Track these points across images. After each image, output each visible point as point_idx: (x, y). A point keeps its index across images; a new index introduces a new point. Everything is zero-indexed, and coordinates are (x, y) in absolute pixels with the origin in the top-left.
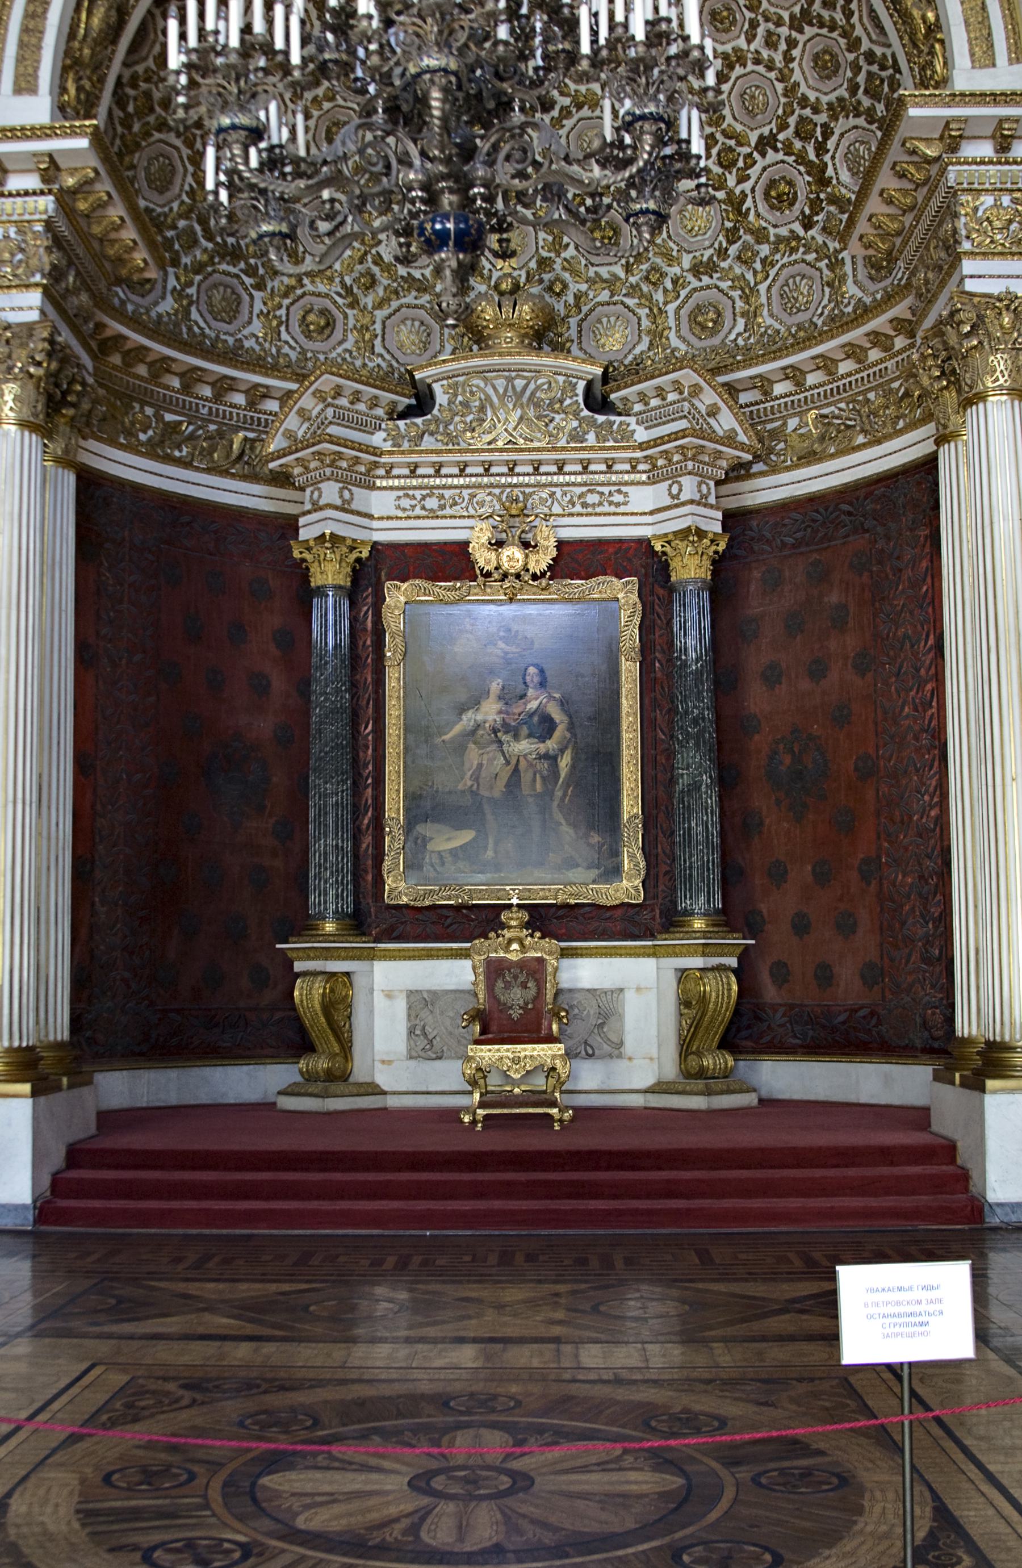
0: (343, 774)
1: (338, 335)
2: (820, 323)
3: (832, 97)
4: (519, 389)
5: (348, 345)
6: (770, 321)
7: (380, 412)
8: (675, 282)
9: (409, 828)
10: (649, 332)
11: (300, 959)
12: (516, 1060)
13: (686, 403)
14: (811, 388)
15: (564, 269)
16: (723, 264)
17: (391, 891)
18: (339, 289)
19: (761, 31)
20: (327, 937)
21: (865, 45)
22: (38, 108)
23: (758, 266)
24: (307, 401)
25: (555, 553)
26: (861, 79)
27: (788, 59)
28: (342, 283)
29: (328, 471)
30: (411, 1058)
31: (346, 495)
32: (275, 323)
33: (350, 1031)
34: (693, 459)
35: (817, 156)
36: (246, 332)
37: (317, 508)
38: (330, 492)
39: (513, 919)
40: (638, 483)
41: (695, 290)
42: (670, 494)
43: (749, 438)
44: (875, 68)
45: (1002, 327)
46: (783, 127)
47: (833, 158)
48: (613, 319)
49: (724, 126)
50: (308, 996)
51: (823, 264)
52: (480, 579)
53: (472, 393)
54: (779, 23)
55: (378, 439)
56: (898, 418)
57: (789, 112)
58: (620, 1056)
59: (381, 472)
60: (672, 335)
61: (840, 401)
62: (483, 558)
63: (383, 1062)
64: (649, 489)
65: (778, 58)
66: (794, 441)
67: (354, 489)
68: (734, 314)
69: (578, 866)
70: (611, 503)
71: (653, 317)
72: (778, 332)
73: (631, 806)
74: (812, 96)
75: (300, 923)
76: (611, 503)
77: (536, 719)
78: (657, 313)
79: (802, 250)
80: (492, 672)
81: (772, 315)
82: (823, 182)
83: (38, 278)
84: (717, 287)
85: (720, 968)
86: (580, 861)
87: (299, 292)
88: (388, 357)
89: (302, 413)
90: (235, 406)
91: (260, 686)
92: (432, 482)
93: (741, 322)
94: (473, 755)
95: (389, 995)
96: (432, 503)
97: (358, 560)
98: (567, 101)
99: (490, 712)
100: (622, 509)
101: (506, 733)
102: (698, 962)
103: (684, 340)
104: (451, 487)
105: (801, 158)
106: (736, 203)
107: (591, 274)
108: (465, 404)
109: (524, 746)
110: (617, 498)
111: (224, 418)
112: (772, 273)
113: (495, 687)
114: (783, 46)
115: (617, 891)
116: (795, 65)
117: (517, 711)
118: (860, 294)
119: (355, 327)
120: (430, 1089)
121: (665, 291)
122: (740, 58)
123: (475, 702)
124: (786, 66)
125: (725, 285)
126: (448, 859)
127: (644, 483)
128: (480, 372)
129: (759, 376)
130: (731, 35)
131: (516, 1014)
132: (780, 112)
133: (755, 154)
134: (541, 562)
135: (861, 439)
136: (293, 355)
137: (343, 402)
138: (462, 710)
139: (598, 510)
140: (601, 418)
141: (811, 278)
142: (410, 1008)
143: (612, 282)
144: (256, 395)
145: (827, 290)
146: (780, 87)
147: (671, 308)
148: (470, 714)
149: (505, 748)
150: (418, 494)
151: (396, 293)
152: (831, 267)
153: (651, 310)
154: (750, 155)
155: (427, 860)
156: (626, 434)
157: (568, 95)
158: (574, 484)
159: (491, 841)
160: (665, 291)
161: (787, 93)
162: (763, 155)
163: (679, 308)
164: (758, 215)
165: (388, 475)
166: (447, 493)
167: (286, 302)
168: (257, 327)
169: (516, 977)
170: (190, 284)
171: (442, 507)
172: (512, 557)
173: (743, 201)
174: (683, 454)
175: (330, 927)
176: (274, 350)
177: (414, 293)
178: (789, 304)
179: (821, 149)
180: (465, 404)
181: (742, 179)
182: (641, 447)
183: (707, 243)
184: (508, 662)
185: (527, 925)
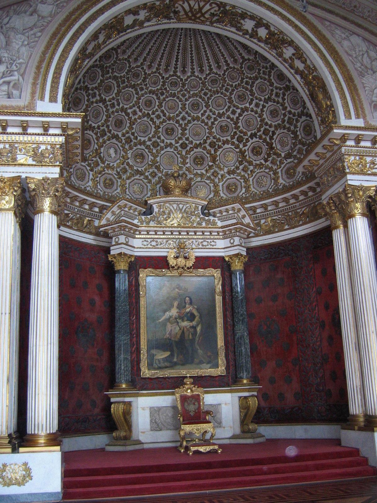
0: (127, 333)
1: (115, 187)
2: (271, 190)
3: (276, 123)
4: (181, 208)
5: (118, 191)
6: (253, 190)
7: (136, 213)
8: (222, 176)
9: (148, 351)
11: (113, 397)
12: (197, 430)
13: (236, 214)
14: (269, 211)
15: (186, 170)
16: (238, 171)
17: (143, 373)
18: (115, 173)
19: (254, 102)
20: (124, 389)
21: (288, 109)
22: (58, 107)
23: (249, 172)
24: (115, 209)
25: (194, 261)
26: (286, 118)
27: (262, 111)
28: (117, 171)
29: (122, 232)
30: (151, 430)
31: (127, 239)
32: (96, 183)
33: (131, 422)
34: (239, 232)
35: (270, 140)
36: (87, 185)
38: (122, 239)
40: (219, 239)
41: (228, 179)
42: (230, 243)
43: (254, 225)
44: (291, 116)
46: (259, 131)
47: (275, 141)
48: (201, 187)
49: (240, 129)
50: (116, 410)
51: (271, 173)
52: (171, 269)
53: (166, 209)
54: (260, 100)
55: (136, 222)
57: (261, 126)
58: (220, 427)
59: (138, 233)
60: (221, 192)
61: (279, 215)
62: (172, 262)
63: (142, 432)
64: (223, 241)
65: (259, 110)
66: (263, 227)
67: (129, 238)
68: (241, 187)
69: (204, 363)
70: (211, 245)
72: (256, 193)
73: (221, 343)
74: (269, 122)
75: (112, 383)
76: (211, 245)
78: (216, 186)
79: (264, 168)
80: (175, 299)
81: (254, 188)
82: (272, 148)
83: (58, 163)
84: (235, 178)
85: (253, 396)
87: (103, 173)
88: (131, 195)
89: (113, 213)
90: (85, 209)
91: (92, 303)
92: (154, 236)
94: (169, 327)
95: (143, 409)
96: (154, 243)
97: (131, 261)
98: (190, 118)
99: (174, 312)
100: (214, 247)
103: (225, 194)
104: (160, 238)
105: (265, 141)
106: (242, 153)
108: (164, 212)
110: (213, 243)
111: (88, 214)
112: (254, 175)
113: (176, 304)
114: (261, 107)
115: (217, 371)
116: (264, 113)
117: (183, 312)
119: (120, 185)
120: (159, 441)
121: (219, 179)
122: (246, 109)
124: (262, 113)
125: (238, 178)
126: (162, 362)
127: (221, 239)
129: (254, 206)
130: (244, 103)
131: (192, 414)
132: (258, 126)
133: (249, 139)
134: (190, 263)
135: (286, 227)
136: (102, 193)
137: (127, 209)
138: (165, 311)
139: (207, 247)
140: (207, 218)
141: (266, 177)
142: (151, 413)
143: (202, 175)
144: (93, 205)
145: (273, 181)
146: (259, 119)
147: (221, 184)
148: (167, 313)
149: (180, 324)
150: (149, 240)
151: (133, 175)
152: (274, 174)
153: (214, 185)
154: (247, 139)
156: (214, 223)
157: (191, 117)
158: (199, 239)
159: (176, 355)
160: (219, 179)
161: (261, 121)
163: (223, 185)
164: (249, 157)
165: (140, 234)
166: (159, 240)
168: (90, 183)
169: (191, 401)
171: (157, 245)
172: (181, 261)
174: (236, 230)
175: (124, 386)
176: (96, 191)
177: (139, 175)
179: (271, 138)
180: (164, 212)
181: (245, 145)
182: (222, 227)
183: (232, 165)
185: (191, 384)
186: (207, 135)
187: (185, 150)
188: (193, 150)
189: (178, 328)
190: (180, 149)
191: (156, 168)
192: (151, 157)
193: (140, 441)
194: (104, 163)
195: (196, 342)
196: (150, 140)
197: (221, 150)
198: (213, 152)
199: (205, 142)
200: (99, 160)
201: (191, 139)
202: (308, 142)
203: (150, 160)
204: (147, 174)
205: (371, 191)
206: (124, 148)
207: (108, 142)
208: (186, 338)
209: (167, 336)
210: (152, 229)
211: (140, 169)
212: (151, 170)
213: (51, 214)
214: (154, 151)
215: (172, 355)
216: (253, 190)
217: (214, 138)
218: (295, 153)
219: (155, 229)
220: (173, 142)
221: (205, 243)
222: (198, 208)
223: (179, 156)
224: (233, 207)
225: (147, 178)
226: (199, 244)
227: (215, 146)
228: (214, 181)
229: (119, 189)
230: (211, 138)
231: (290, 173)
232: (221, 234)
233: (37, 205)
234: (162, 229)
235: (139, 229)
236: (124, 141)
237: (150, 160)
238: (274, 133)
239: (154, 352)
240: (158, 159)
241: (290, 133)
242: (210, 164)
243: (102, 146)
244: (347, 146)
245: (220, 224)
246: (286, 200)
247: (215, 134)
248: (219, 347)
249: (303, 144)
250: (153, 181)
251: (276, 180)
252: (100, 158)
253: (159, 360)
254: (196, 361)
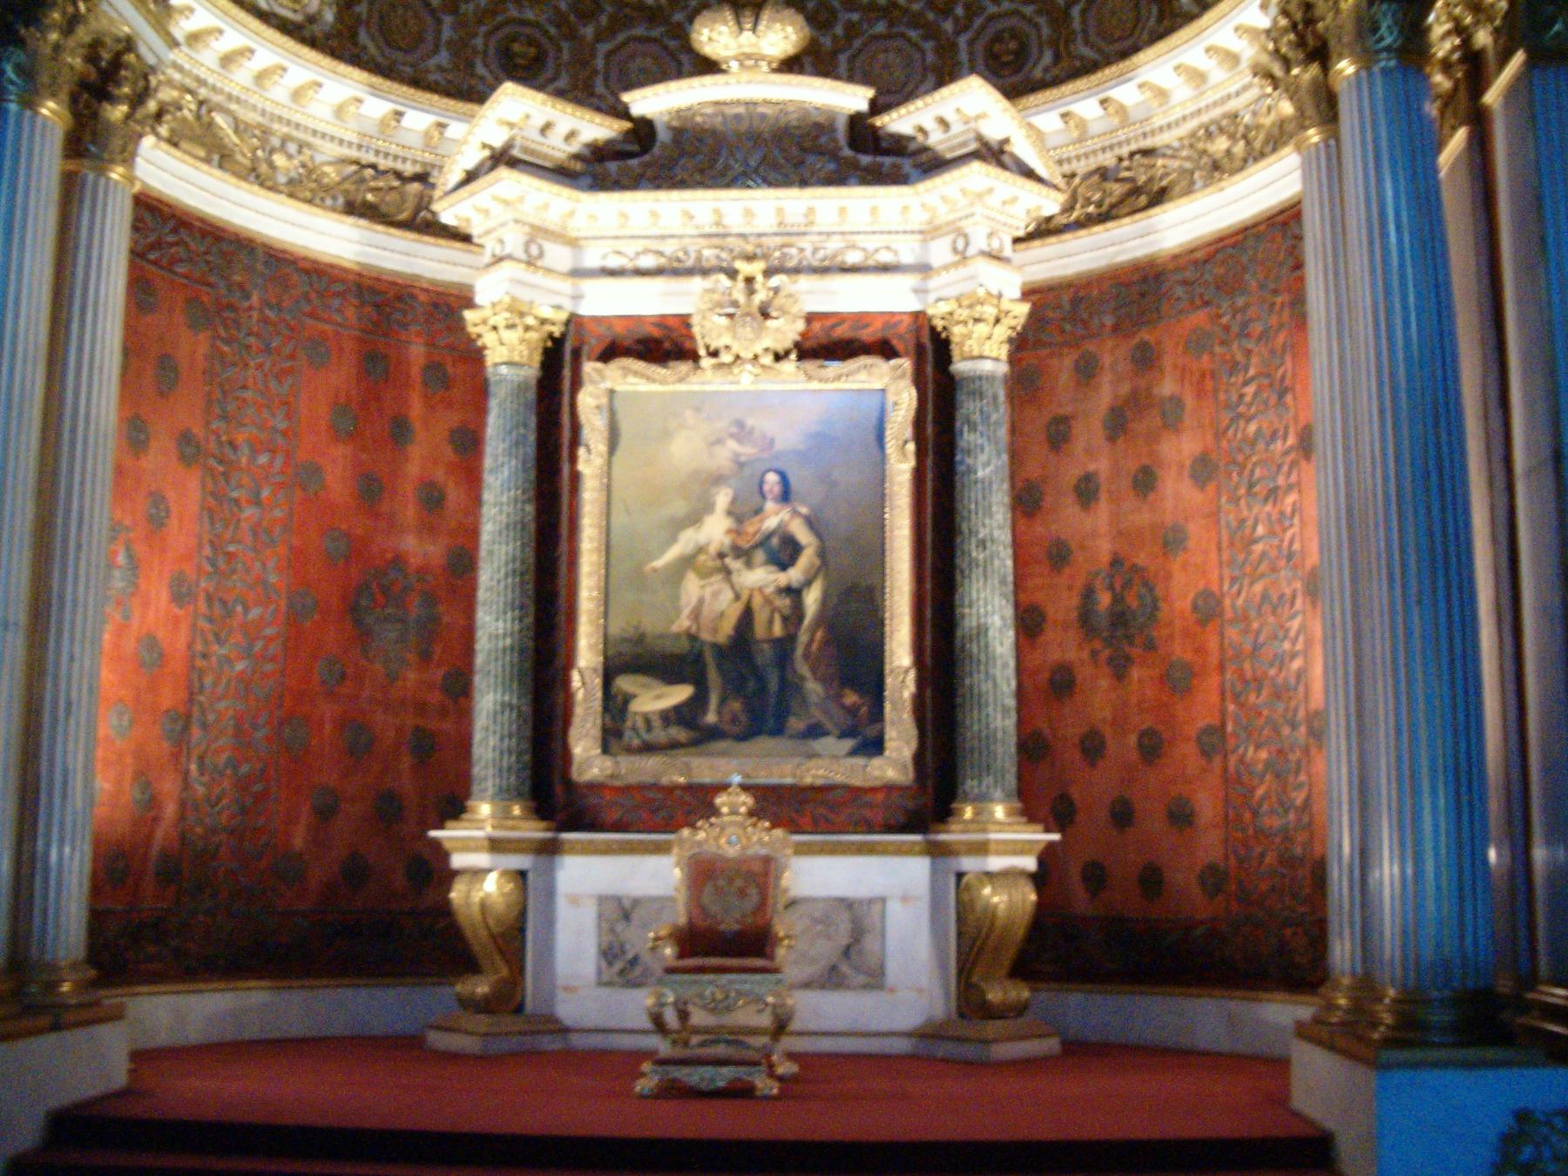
62: (710, 330)
69: (825, 734)
77: (775, 541)
80: (718, 480)
86: (829, 725)
94: (692, 588)
99: (715, 530)
101: (737, 557)
109: (760, 577)
113: (723, 498)
117: (751, 529)
123: (694, 518)
126: (657, 723)
138: (677, 526)
149: (735, 578)
155: (629, 723)
184: (741, 465)
189: (728, 595)
193: (557, 1021)
195: (799, 651)
208: (760, 630)
209: (683, 623)
215: (698, 702)
239: (624, 683)
254: (795, 724)
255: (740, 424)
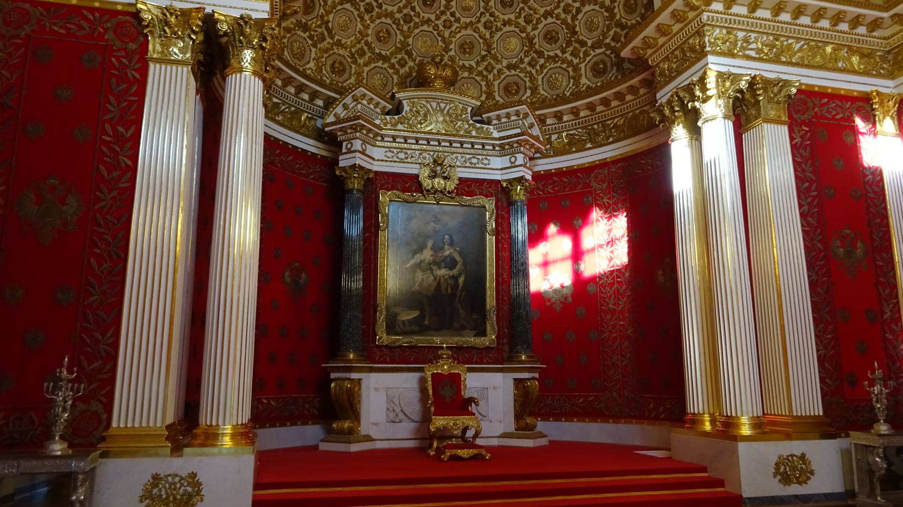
1: (346, 76)
2: (568, 94)
6: (542, 92)
7: (378, 110)
8: (499, 71)
10: (486, 92)
11: (334, 372)
16: (521, 66)
17: (380, 339)
20: (351, 361)
23: (538, 68)
24: (348, 100)
29: (358, 134)
36: (308, 66)
37: (349, 151)
38: (357, 145)
39: (445, 353)
45: (724, 86)
46: (557, 7)
51: (570, 69)
55: (377, 122)
56: (610, 137)
60: (496, 94)
62: (427, 183)
63: (374, 424)
66: (555, 144)
71: (487, 85)
78: (489, 85)
80: (428, 237)
82: (575, 33)
85: (534, 378)
89: (345, 107)
93: (529, 93)
95: (376, 389)
96: (402, 156)
97: (368, 178)
102: (525, 375)
106: (531, 40)
107: (461, 63)
109: (443, 272)
110: (485, 162)
112: (545, 71)
113: (430, 244)
118: (588, 83)
125: (522, 75)
128: (426, 98)
134: (451, 185)
135: (589, 145)
136: (328, 81)
140: (478, 125)
143: (470, 69)
144: (314, 95)
150: (395, 151)
156: (488, 132)
162: (546, 19)
163: (499, 85)
164: (540, 46)
165: (382, 140)
167: (325, 55)
168: (312, 65)
170: (284, 37)
171: (407, 158)
172: (439, 182)
173: (533, 39)
178: (551, 85)
179: (574, 18)
180: (418, 112)
181: (533, 30)
182: (500, 139)
184: (436, 232)
186: (482, 10)
187: (449, 31)
188: (460, 32)
190: (441, 28)
191: (406, 53)
192: (400, 37)
194: (332, 38)
196: (400, 11)
197: (499, 34)
198: (488, 36)
199: (479, 21)
200: (326, 33)
201: (458, 15)
202: (629, 23)
203: (398, 40)
204: (393, 61)
205: (743, 83)
206: (362, 19)
207: (339, 7)
208: (443, 291)
209: (416, 287)
210: (402, 133)
211: (383, 53)
212: (399, 56)
213: (253, 77)
214: (405, 28)
215: (421, 317)
216: (542, 92)
217: (492, 15)
218: (607, 41)
219: (406, 134)
220: (433, 17)
221: (474, 161)
222: (466, 109)
223: (440, 39)
224: (518, 111)
225: (392, 66)
226: (465, 161)
227: (491, 28)
228: (486, 77)
229: (353, 79)
230: (487, 14)
231: (598, 71)
232: (497, 148)
233: (229, 61)
234: (414, 135)
235: (383, 132)
236: (362, 9)
237: (398, 40)
238: (579, 11)
240: (410, 41)
241: (603, 10)
242: (483, 53)
243: (331, 12)
244: (711, 12)
245: (496, 134)
246: (591, 107)
247: (493, 9)
248: (488, 307)
249: (622, 26)
250: (402, 71)
251: (576, 79)
252: (327, 28)
253: (403, 322)
255: (436, 217)
